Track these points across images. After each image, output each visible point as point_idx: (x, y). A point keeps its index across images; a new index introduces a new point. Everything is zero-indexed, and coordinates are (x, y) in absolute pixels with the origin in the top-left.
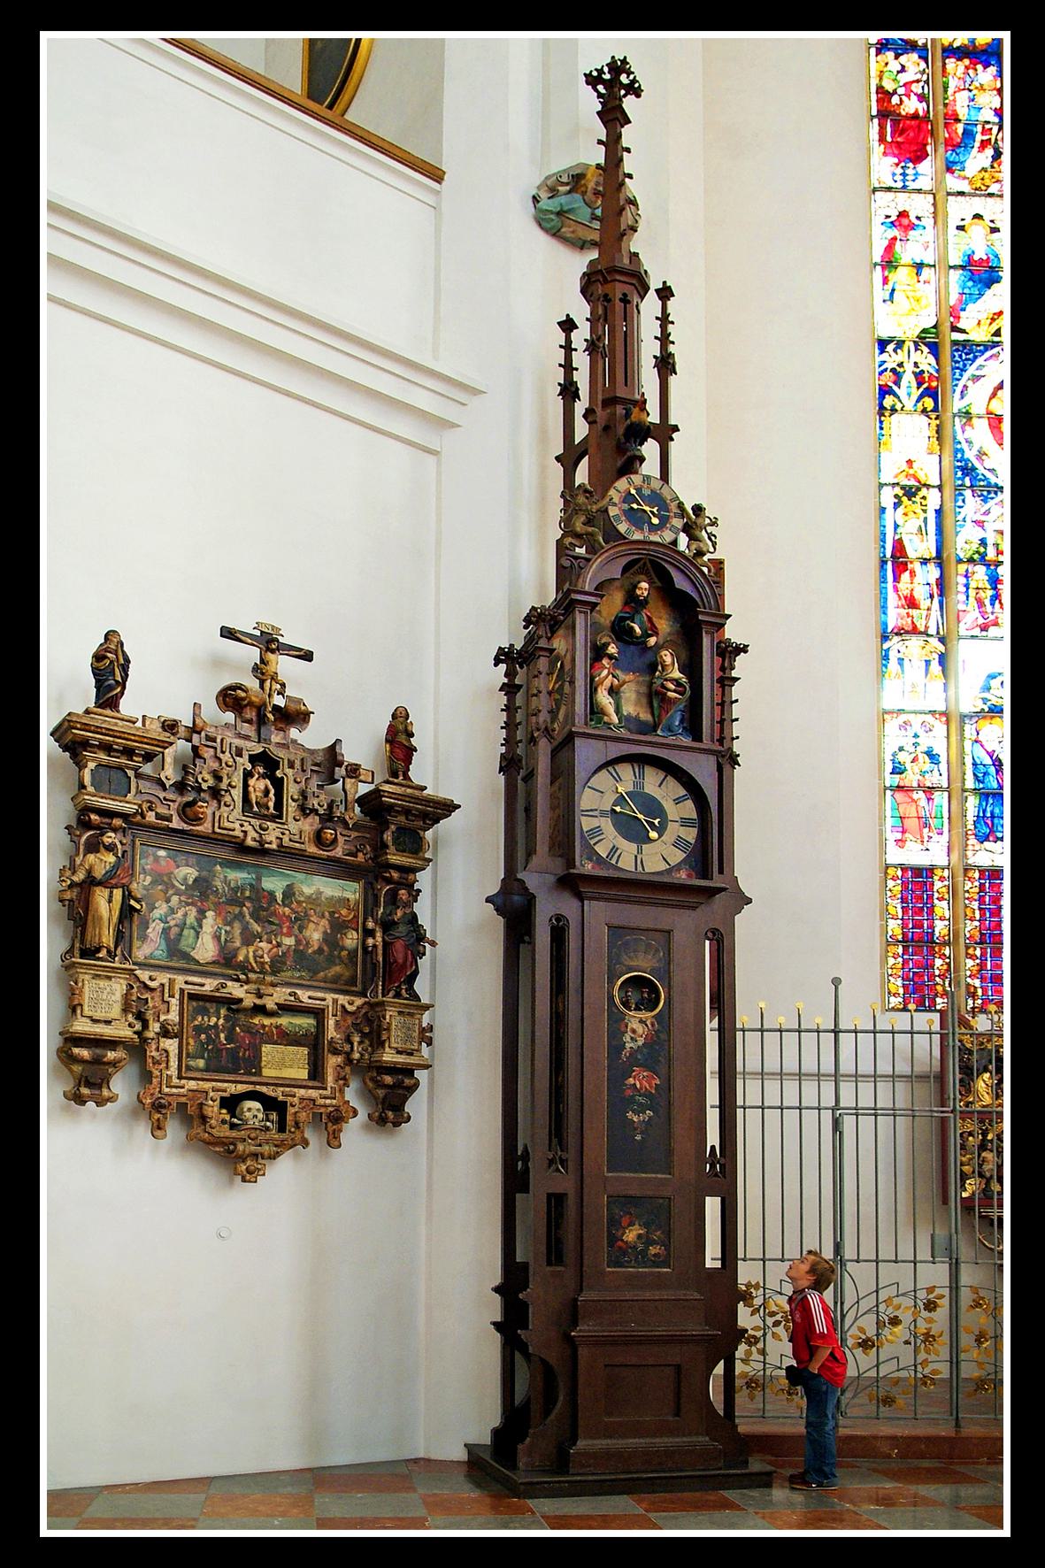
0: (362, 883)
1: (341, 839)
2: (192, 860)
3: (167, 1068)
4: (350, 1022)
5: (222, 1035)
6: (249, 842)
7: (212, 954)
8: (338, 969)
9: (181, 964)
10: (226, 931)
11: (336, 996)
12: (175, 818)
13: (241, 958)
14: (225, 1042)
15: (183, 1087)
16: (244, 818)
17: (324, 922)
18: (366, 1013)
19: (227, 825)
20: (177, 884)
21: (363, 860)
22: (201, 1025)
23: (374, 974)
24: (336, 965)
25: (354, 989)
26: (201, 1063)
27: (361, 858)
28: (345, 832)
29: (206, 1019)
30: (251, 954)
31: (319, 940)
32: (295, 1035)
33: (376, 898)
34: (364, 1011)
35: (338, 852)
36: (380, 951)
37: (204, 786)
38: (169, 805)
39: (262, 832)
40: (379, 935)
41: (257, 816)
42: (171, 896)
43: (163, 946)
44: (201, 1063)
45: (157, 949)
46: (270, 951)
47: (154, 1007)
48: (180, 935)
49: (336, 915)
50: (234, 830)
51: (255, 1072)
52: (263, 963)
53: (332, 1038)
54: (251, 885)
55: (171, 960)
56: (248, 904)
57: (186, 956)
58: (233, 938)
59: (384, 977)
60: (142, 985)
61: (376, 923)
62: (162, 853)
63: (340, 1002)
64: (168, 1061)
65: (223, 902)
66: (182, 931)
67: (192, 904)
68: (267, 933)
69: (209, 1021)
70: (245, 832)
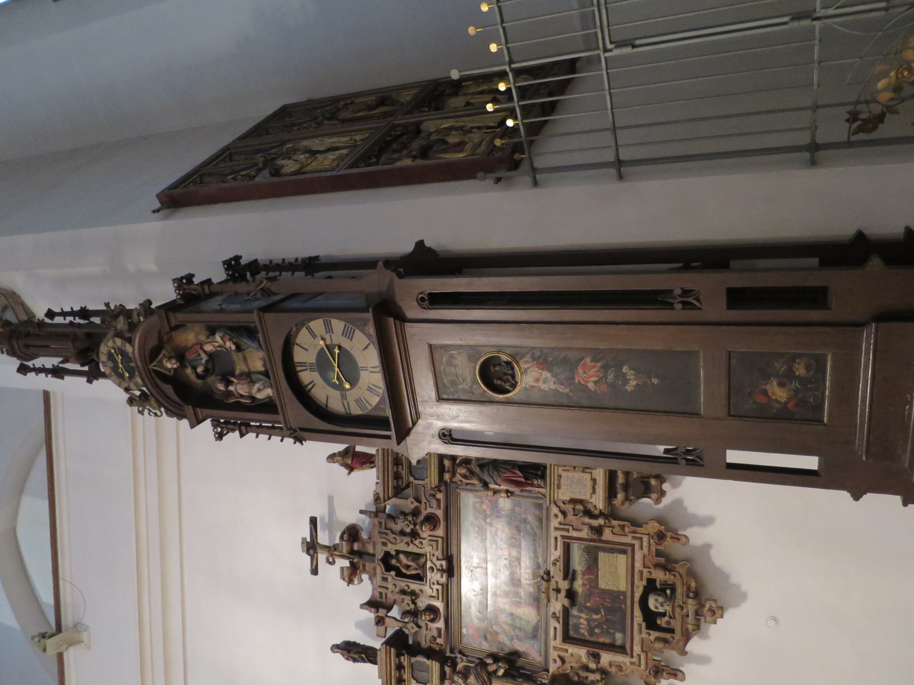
3: (625, 664)
5: (595, 617)
11: (552, 528)
14: (600, 615)
15: (639, 656)
19: (435, 594)
35: (440, 513)
44: (619, 636)
47: (577, 662)
48: (520, 629)
50: (437, 590)
53: (588, 536)
57: (536, 629)
63: (557, 525)
66: (516, 627)
69: (584, 624)
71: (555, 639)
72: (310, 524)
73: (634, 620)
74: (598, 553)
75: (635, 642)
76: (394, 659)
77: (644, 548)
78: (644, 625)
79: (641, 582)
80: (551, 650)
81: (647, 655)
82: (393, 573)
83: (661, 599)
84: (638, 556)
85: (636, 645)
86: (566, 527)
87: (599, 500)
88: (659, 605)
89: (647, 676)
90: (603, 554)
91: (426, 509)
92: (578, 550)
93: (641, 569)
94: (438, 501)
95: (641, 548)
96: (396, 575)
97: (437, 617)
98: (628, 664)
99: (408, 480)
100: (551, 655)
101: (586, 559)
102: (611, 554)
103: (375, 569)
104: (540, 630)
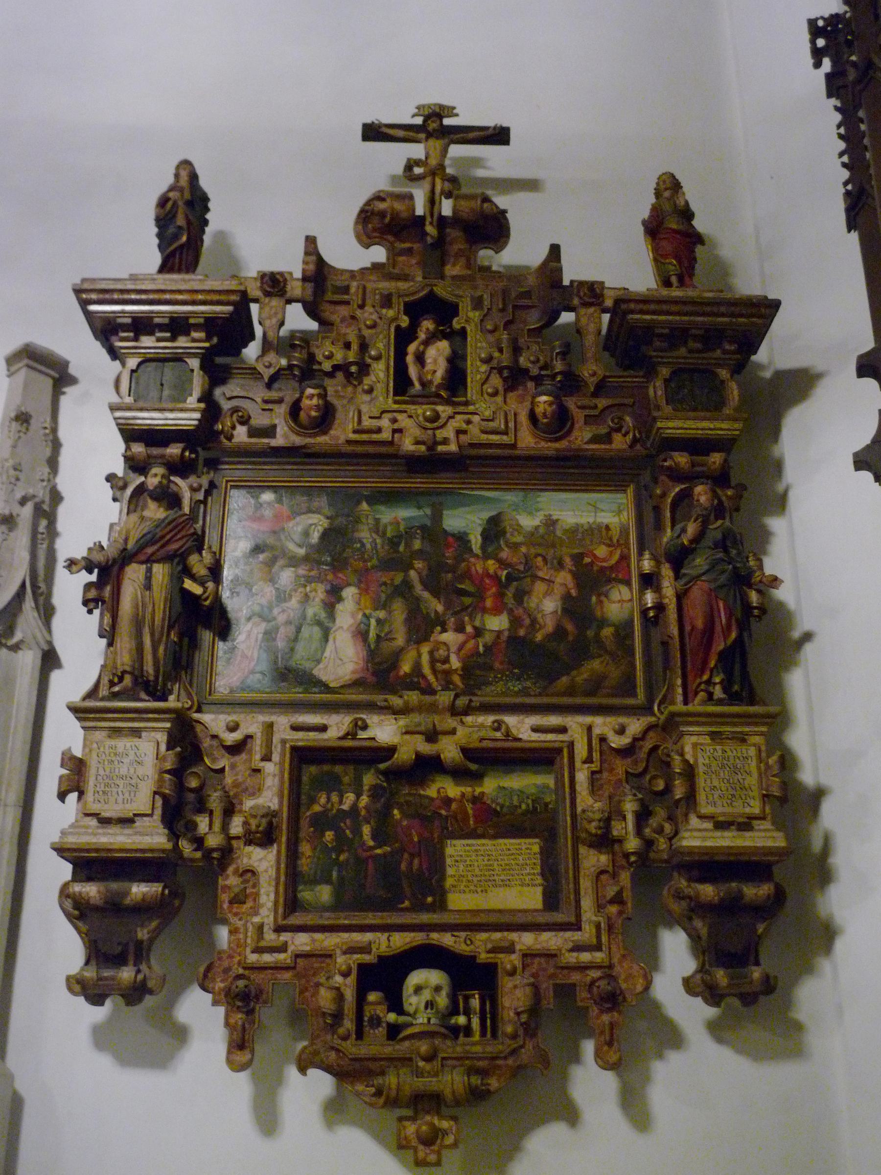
1: (579, 416)
5: (366, 830)
6: (408, 445)
8: (596, 665)
9: (297, 694)
10: (379, 621)
11: (588, 719)
13: (406, 668)
14: (371, 843)
15: (282, 948)
16: (396, 407)
17: (564, 578)
19: (367, 423)
20: (291, 546)
22: (325, 812)
24: (593, 658)
25: (630, 701)
27: (619, 442)
28: (586, 401)
29: (335, 798)
30: (425, 659)
31: (556, 612)
32: (513, 814)
34: (648, 745)
39: (429, 425)
43: (264, 666)
44: (324, 893)
45: (253, 672)
46: (461, 647)
47: (236, 785)
49: (587, 560)
50: (379, 430)
51: (433, 904)
52: (448, 673)
53: (584, 811)
54: (423, 528)
56: (419, 564)
58: (390, 632)
62: (268, 497)
63: (596, 731)
65: (373, 567)
66: (299, 630)
67: (319, 579)
68: (455, 613)
69: (341, 802)
71: (295, 728)
73: (378, 934)
74: (536, 837)
75: (318, 936)
77: (575, 954)
79: (482, 949)
80: (263, 718)
81: (287, 968)
82: (405, 322)
83: (442, 1001)
84: (550, 940)
85: (314, 941)
86: (596, 756)
87: (704, 839)
88: (426, 995)
89: (227, 970)
90: (536, 849)
93: (518, 947)
94: (607, 438)
95: (578, 948)
96: (398, 328)
97: (300, 425)
98: (257, 919)
99: (659, 363)
100: (249, 717)
101: (516, 807)
102: (538, 869)
103: (405, 278)
104: (301, 690)
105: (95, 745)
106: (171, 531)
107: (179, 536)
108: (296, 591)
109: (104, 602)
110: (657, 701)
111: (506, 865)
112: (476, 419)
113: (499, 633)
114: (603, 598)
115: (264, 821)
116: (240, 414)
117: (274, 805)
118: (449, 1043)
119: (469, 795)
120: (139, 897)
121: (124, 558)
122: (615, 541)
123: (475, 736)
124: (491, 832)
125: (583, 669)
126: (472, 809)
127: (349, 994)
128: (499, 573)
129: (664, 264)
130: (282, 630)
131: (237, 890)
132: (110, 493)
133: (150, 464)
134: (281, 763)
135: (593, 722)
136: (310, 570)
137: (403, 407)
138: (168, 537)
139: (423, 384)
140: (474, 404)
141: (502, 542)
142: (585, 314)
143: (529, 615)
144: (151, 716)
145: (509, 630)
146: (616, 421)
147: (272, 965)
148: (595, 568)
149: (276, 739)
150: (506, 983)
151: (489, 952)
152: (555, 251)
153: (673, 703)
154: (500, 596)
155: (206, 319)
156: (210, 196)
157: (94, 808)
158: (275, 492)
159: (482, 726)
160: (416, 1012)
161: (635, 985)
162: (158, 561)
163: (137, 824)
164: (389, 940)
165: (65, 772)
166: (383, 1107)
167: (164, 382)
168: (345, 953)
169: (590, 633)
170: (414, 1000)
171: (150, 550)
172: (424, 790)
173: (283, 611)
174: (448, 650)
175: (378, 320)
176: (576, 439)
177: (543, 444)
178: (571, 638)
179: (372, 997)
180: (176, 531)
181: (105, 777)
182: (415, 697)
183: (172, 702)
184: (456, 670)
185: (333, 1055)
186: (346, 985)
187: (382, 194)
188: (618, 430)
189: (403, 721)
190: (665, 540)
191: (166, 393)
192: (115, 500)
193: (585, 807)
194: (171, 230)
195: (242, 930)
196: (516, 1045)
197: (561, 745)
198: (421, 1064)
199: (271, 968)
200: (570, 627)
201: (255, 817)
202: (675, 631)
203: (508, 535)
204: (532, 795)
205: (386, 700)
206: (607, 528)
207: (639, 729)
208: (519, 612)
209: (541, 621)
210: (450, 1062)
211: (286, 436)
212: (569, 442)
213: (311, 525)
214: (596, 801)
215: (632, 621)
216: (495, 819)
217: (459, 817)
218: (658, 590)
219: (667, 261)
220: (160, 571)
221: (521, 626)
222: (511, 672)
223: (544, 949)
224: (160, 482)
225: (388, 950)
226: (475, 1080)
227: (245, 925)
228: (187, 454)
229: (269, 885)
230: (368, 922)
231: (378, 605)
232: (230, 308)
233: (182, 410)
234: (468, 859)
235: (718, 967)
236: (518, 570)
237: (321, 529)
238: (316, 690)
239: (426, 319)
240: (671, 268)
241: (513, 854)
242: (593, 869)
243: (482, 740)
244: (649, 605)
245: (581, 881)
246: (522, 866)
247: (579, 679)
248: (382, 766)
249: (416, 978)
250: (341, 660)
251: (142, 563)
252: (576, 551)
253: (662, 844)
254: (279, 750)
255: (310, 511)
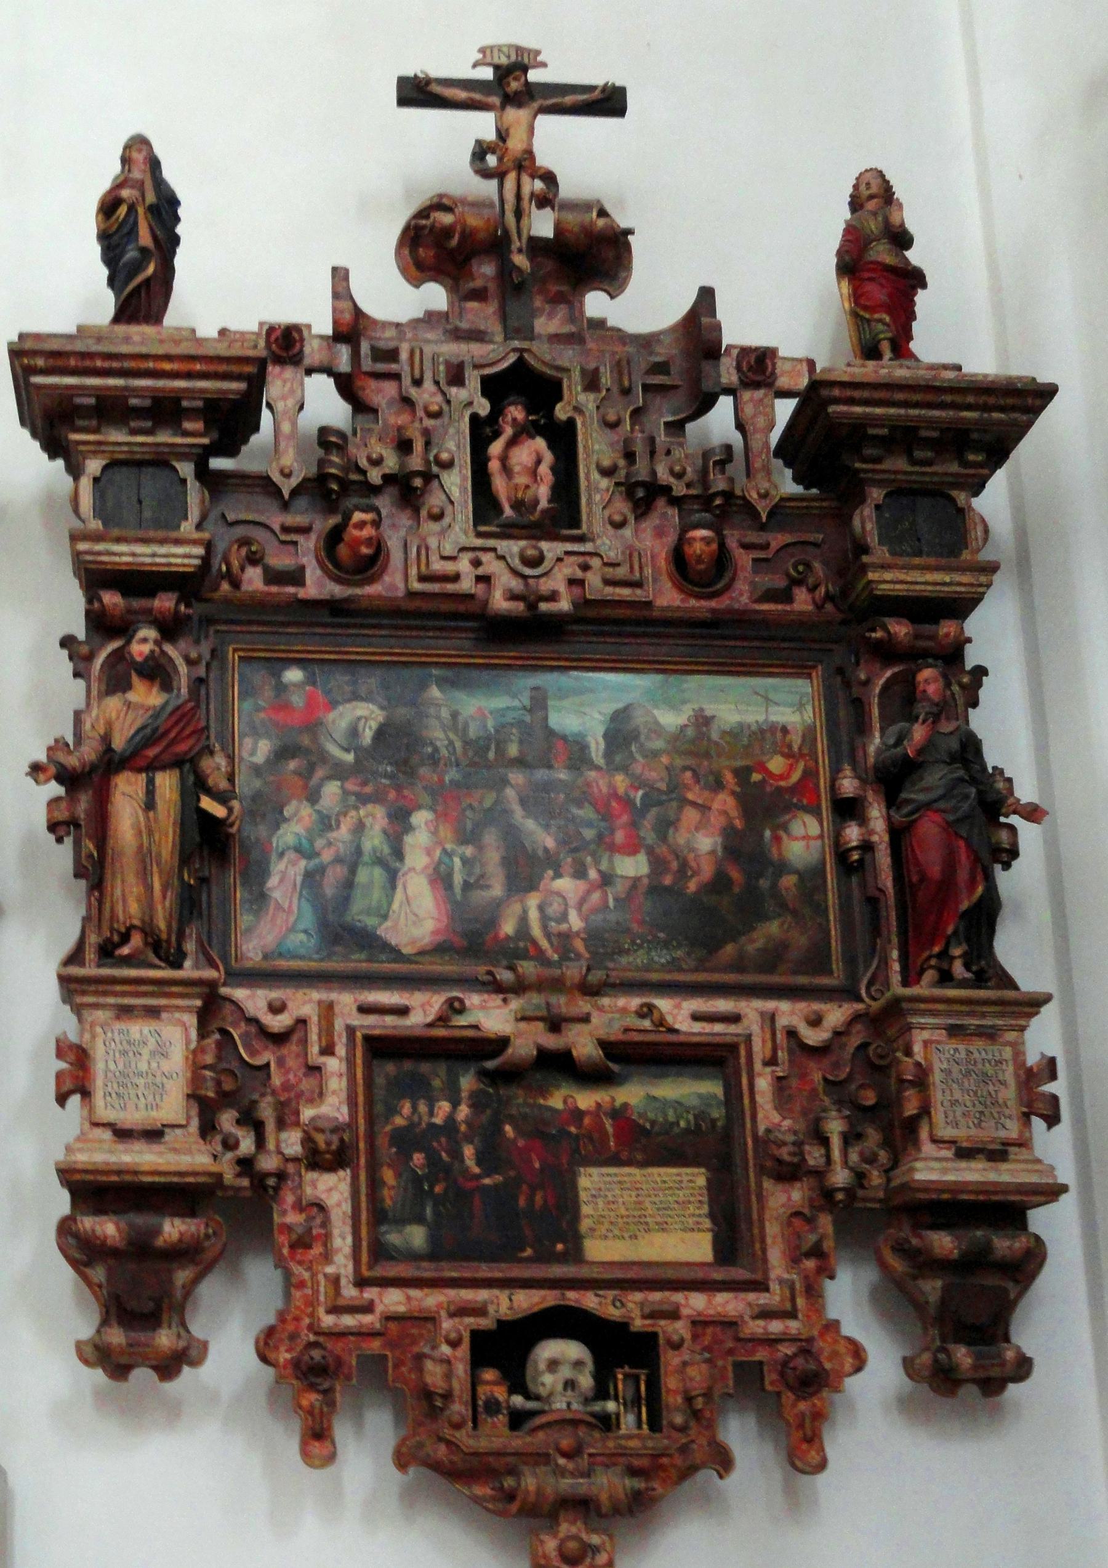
0: (818, 673)
1: (744, 559)
2: (371, 681)
3: (327, 1257)
4: (817, 1077)
5: (468, 1151)
6: (499, 603)
7: (429, 925)
8: (774, 928)
10: (465, 861)
11: (770, 1005)
12: (313, 574)
13: (508, 928)
14: (477, 1170)
15: (368, 1308)
16: (479, 542)
17: (725, 802)
18: (864, 1046)
19: (438, 566)
21: (810, 608)
22: (412, 1126)
23: (876, 928)
26: (417, 1236)
27: (802, 601)
28: (753, 537)
29: (423, 1108)
30: (534, 915)
31: (713, 852)
32: (667, 1133)
33: (859, 705)
34: (855, 1041)
36: (883, 859)
37: (375, 476)
38: (295, 543)
39: (528, 571)
40: (876, 814)
41: (508, 531)
42: (320, 786)
44: (417, 1236)
45: (292, 929)
47: (286, 1087)
48: (349, 884)
49: (756, 777)
50: (456, 578)
53: (768, 1131)
54: (520, 723)
55: (329, 957)
56: (517, 777)
58: (482, 876)
59: (903, 933)
60: (253, 1029)
61: (863, 781)
63: (782, 1022)
64: (327, 1238)
66: (353, 871)
67: (377, 798)
69: (431, 1113)
70: (484, 579)
71: (365, 1009)
72: (605, 88)
73: (496, 1292)
74: (698, 1165)
75: (414, 1293)
76: (202, 391)
77: (761, 1323)
78: (485, 1323)
80: (316, 995)
82: (483, 407)
83: (586, 1381)
84: (727, 1304)
85: (409, 1298)
88: (566, 1372)
89: (293, 1337)
90: (701, 1181)
91: (746, 547)
92: (700, 1096)
93: (685, 1312)
94: (785, 596)
95: (766, 1314)
96: (475, 418)
97: (337, 564)
98: (330, 1270)
100: (300, 994)
101: (672, 1124)
102: (705, 1209)
103: (477, 336)
104: (363, 956)
105: (99, 1030)
106: (177, 723)
107: (187, 732)
108: (345, 815)
109: (77, 826)
110: (865, 981)
111: (661, 1202)
112: (595, 562)
113: (636, 881)
114: (782, 833)
115: (335, 1139)
116: (254, 548)
117: (342, 1114)
118: (597, 1435)
119: (606, 1106)
120: (175, 1236)
121: (109, 762)
122: (796, 748)
123: (617, 1026)
124: (639, 1157)
125: (755, 935)
126: (613, 1126)
127: (461, 1369)
128: (632, 794)
129: (868, 321)
130: (329, 872)
131: (300, 1230)
132: (69, 667)
133: (132, 623)
134: (350, 1061)
135: (777, 1009)
136: (364, 783)
137: (491, 543)
138: (172, 735)
139: (517, 505)
140: (593, 540)
141: (633, 748)
142: (751, 400)
143: (677, 857)
144: (175, 989)
145: (648, 876)
146: (801, 568)
147: (354, 1330)
148: (768, 789)
149: (339, 1025)
150: (671, 1360)
151: (644, 1317)
152: (706, 296)
153: (887, 984)
154: (634, 825)
155: (207, 401)
156: (180, 196)
157: (105, 1113)
158: (304, 669)
159: (624, 1011)
160: (551, 1394)
161: (842, 1365)
162: (163, 768)
163: (167, 1138)
164: (511, 1300)
165: (63, 1065)
166: (514, 1516)
167: (142, 496)
168: (452, 1315)
169: (764, 883)
170: (548, 1379)
171: (152, 752)
172: (545, 1098)
173: (330, 844)
174: (566, 905)
175: (445, 407)
176: (741, 595)
177: (693, 602)
178: (736, 890)
179: (489, 1375)
180: (182, 724)
181: (117, 1074)
182: (532, 969)
183: (188, 970)
184: (578, 934)
185: (442, 1449)
186: (455, 1358)
187: (445, 201)
188: (799, 582)
189: (515, 1004)
190: (871, 750)
191: (147, 514)
192: (77, 675)
193: (770, 1126)
194: (131, 254)
195: (309, 1284)
196: (684, 1441)
197: (735, 1039)
198: (562, 1461)
199: (352, 1334)
200: (735, 874)
201: (321, 1131)
202: (887, 880)
203: (642, 737)
204: (694, 1108)
205: (490, 973)
206: (785, 730)
207: (842, 1019)
208: (661, 850)
209: (693, 864)
210: (599, 1459)
211: (320, 585)
212: (731, 598)
213: (359, 719)
214: (784, 1118)
215: (824, 864)
216: (644, 1141)
217: (596, 1136)
218: (863, 821)
219: (877, 316)
220: (167, 783)
221: (667, 870)
222: (655, 937)
223: (719, 1314)
224: (152, 652)
225: (508, 1312)
226: (638, 1484)
227: (313, 1276)
228: (182, 608)
229: (344, 1223)
230: (481, 1275)
231: (464, 839)
232: (241, 386)
233: (178, 542)
234: (609, 1194)
235: (955, 1342)
236: (658, 790)
237: (374, 725)
238: (383, 957)
239: (510, 404)
240: (880, 327)
241: (670, 1188)
242: (782, 1210)
243: (627, 1030)
244: (854, 844)
245: (767, 1224)
246: (685, 1204)
247: (750, 948)
248: (490, 1064)
249: (550, 1349)
250: (416, 915)
251: (140, 770)
252: (739, 763)
253: (876, 1178)
254: (344, 1040)
255: (356, 697)
